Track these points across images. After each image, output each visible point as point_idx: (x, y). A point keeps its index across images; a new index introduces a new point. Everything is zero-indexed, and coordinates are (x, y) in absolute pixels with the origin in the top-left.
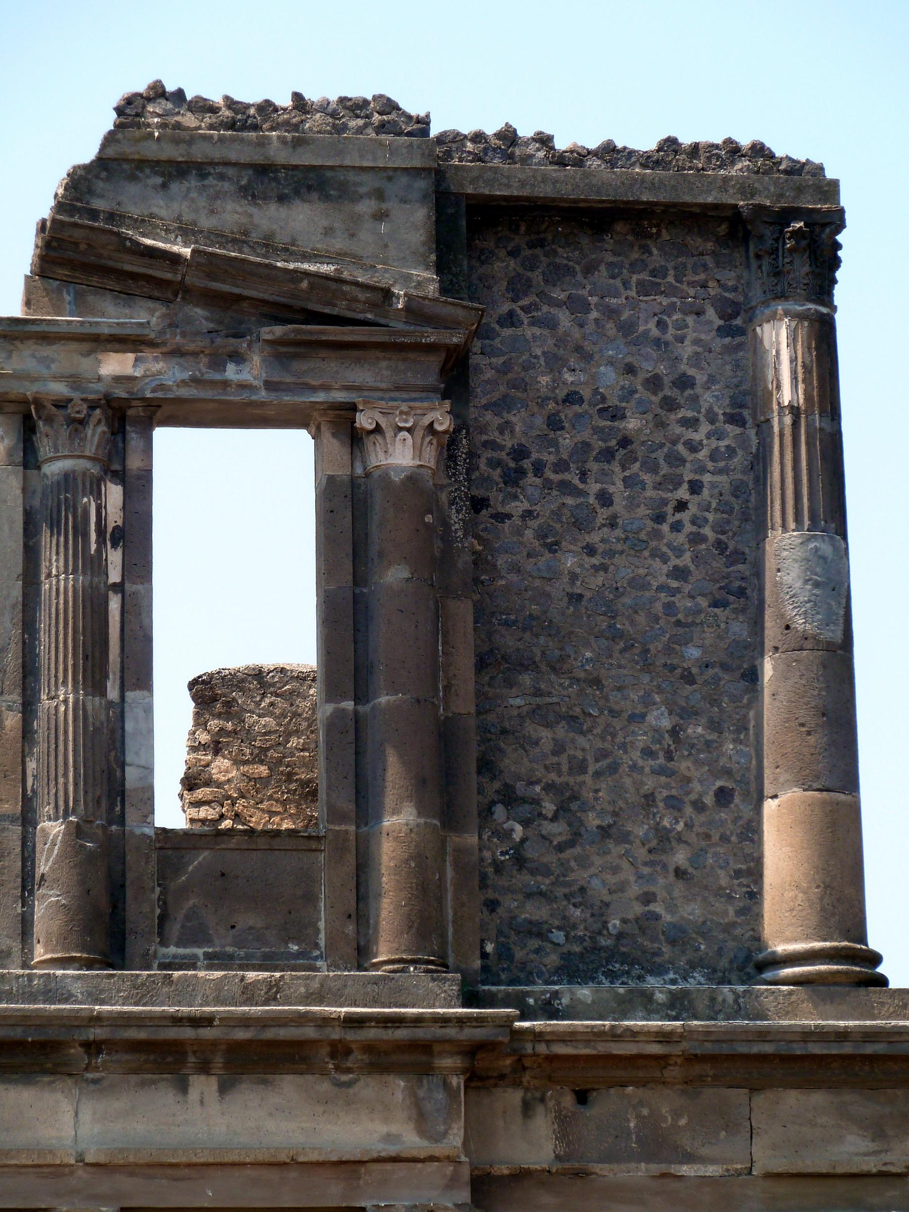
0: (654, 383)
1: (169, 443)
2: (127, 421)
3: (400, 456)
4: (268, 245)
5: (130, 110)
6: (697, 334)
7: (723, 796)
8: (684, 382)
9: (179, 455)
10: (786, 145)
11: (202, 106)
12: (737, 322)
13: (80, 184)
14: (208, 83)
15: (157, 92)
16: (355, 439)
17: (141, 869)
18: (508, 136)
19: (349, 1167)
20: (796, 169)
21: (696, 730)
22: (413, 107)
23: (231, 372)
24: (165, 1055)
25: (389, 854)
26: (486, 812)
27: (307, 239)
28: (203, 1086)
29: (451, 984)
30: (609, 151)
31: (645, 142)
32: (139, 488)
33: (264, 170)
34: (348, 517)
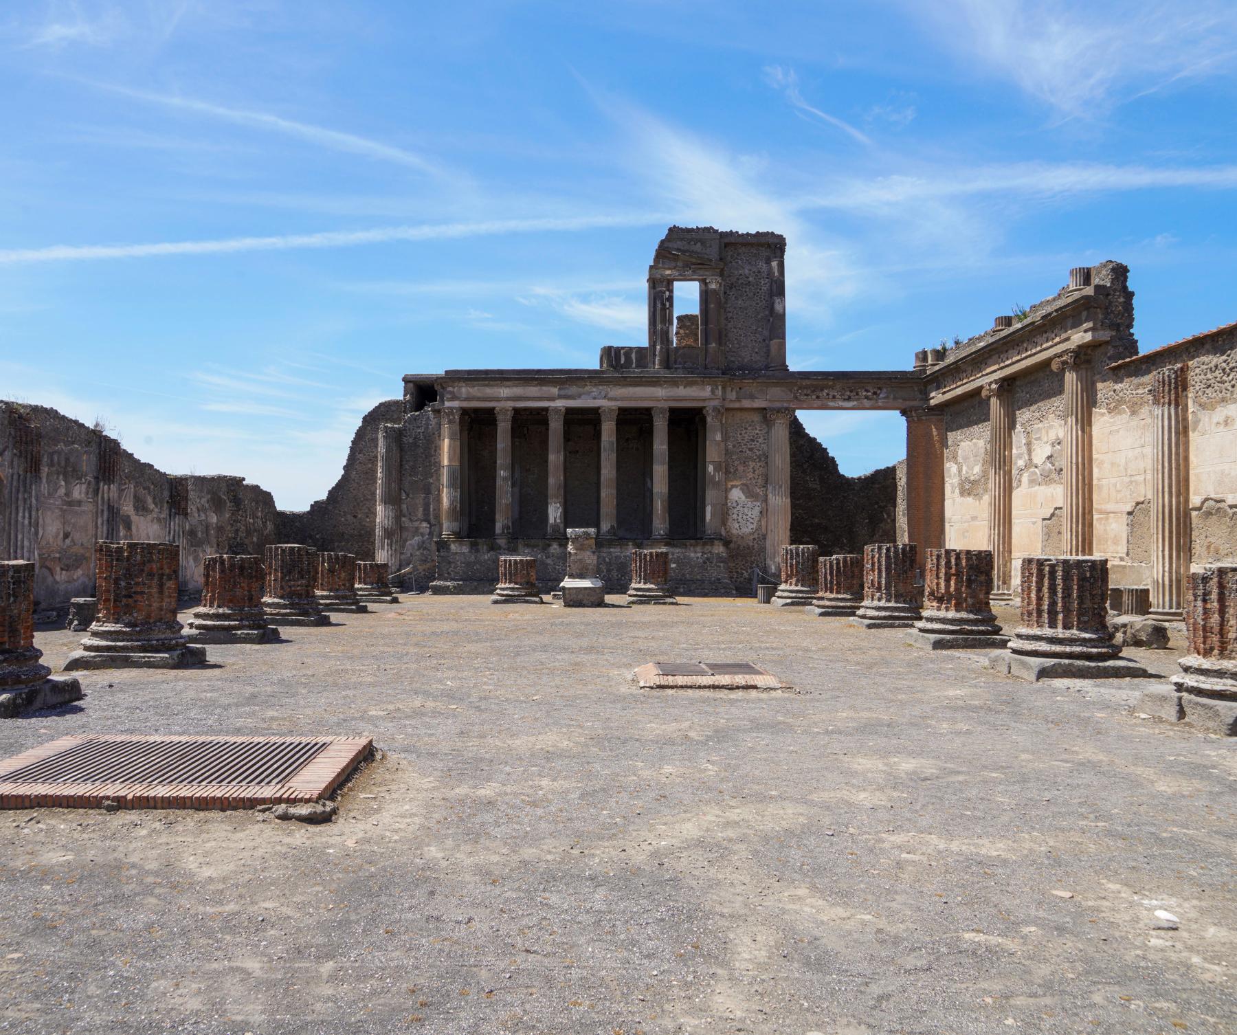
1: (676, 284)
2: (669, 283)
3: (713, 286)
5: (670, 230)
6: (763, 266)
9: (677, 285)
10: (777, 232)
12: (768, 261)
13: (662, 242)
14: (682, 224)
16: (706, 284)
19: (704, 400)
24: (674, 383)
28: (681, 388)
30: (748, 234)
31: (753, 232)
32: (671, 291)
33: (692, 240)
34: (705, 296)
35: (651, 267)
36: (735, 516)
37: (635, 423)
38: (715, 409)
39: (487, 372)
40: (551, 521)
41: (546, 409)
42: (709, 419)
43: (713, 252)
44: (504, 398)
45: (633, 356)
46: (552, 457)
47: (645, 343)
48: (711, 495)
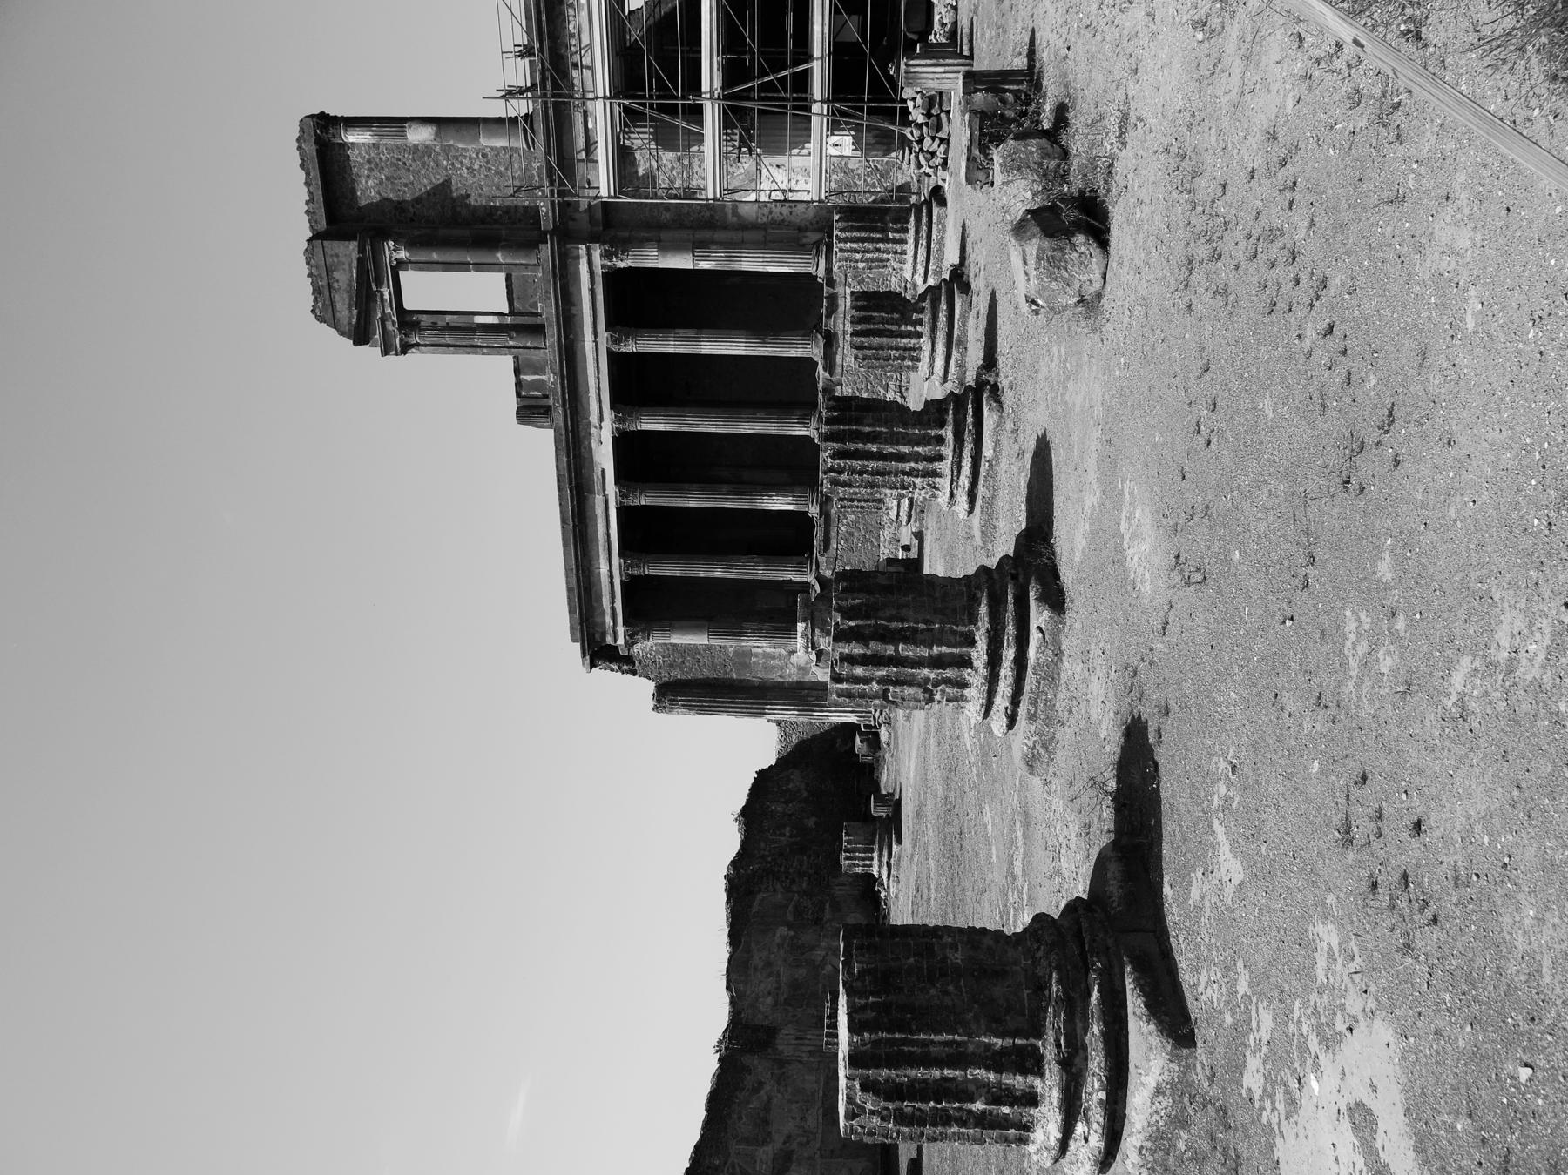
0: (371, 170)
4: (350, 285)
5: (321, 319)
7: (484, 156)
8: (369, 161)
11: (315, 300)
13: (342, 334)
15: (313, 311)
17: (520, 320)
18: (307, 212)
20: (302, 130)
21: (466, 162)
22: (305, 245)
23: (386, 296)
25: (509, 261)
26: (496, 222)
27: (346, 276)
29: (541, 246)
30: (307, 184)
31: (302, 174)
33: (330, 286)
35: (385, 352)
36: (785, 210)
37: (635, 383)
38: (607, 255)
39: (569, 590)
40: (790, 508)
41: (621, 510)
42: (622, 265)
43: (348, 251)
44: (609, 568)
45: (529, 378)
46: (692, 504)
47: (507, 362)
48: (749, 263)
